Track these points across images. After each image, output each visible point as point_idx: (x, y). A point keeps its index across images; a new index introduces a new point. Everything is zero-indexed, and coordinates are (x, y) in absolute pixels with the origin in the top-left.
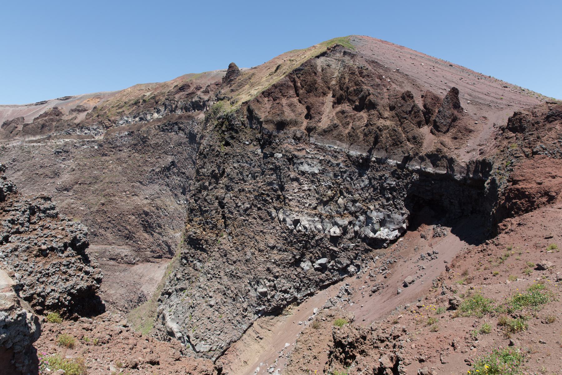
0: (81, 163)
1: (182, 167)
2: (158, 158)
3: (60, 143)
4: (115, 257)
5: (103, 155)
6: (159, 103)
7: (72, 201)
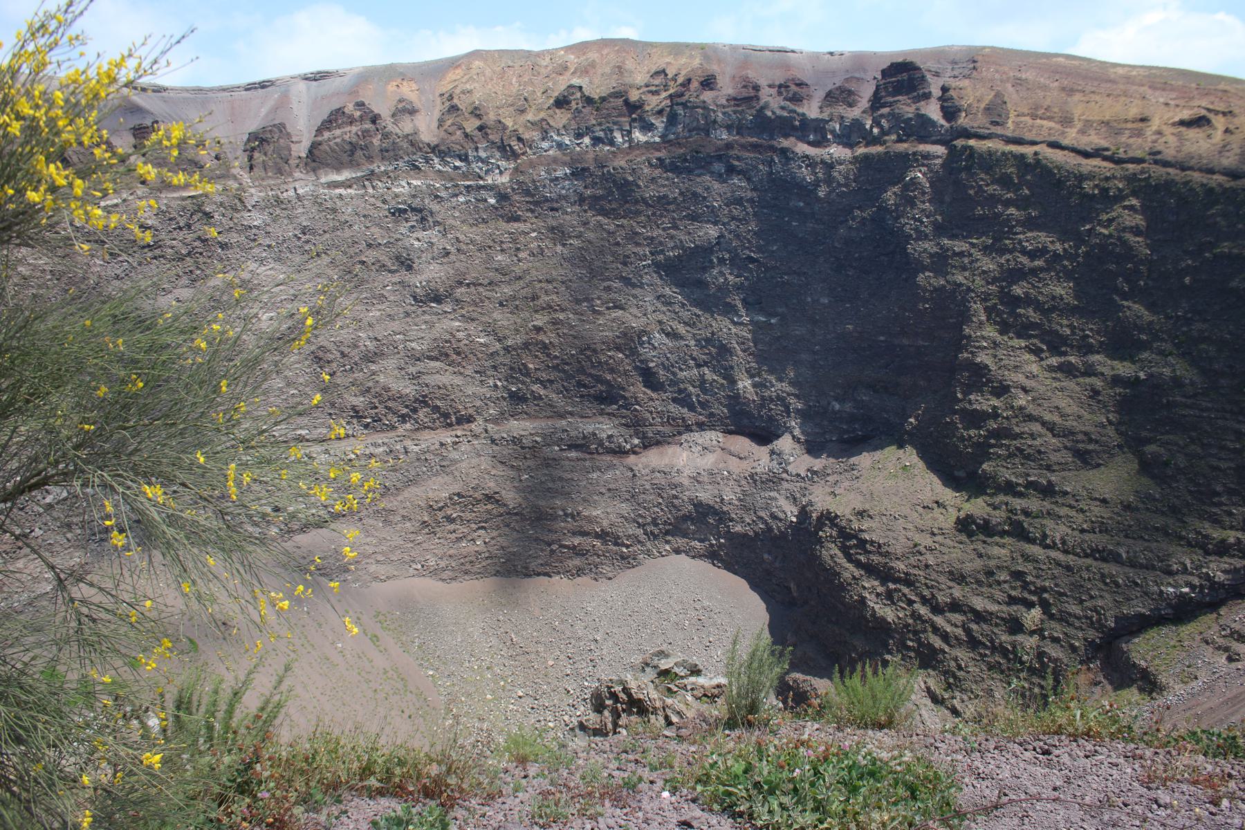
0: (462, 237)
1: (748, 248)
2: (669, 228)
3: (401, 189)
4: (583, 442)
5: (508, 222)
6: (647, 108)
7: (457, 324)
